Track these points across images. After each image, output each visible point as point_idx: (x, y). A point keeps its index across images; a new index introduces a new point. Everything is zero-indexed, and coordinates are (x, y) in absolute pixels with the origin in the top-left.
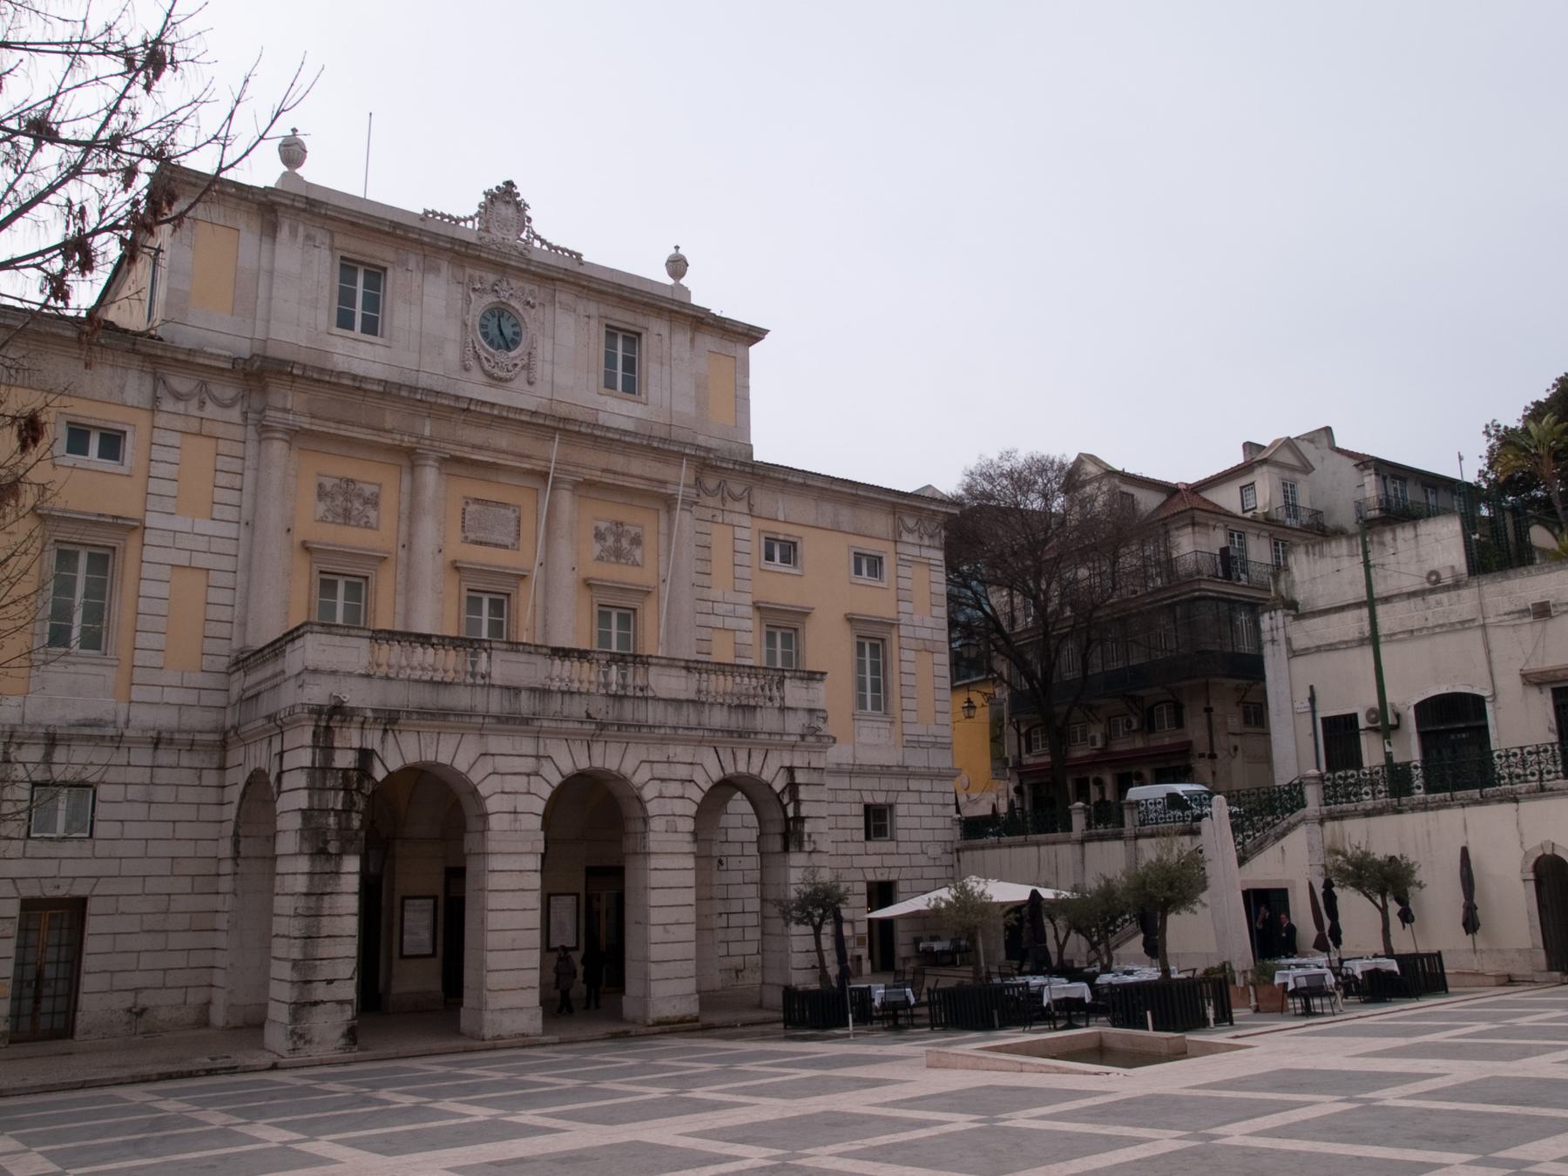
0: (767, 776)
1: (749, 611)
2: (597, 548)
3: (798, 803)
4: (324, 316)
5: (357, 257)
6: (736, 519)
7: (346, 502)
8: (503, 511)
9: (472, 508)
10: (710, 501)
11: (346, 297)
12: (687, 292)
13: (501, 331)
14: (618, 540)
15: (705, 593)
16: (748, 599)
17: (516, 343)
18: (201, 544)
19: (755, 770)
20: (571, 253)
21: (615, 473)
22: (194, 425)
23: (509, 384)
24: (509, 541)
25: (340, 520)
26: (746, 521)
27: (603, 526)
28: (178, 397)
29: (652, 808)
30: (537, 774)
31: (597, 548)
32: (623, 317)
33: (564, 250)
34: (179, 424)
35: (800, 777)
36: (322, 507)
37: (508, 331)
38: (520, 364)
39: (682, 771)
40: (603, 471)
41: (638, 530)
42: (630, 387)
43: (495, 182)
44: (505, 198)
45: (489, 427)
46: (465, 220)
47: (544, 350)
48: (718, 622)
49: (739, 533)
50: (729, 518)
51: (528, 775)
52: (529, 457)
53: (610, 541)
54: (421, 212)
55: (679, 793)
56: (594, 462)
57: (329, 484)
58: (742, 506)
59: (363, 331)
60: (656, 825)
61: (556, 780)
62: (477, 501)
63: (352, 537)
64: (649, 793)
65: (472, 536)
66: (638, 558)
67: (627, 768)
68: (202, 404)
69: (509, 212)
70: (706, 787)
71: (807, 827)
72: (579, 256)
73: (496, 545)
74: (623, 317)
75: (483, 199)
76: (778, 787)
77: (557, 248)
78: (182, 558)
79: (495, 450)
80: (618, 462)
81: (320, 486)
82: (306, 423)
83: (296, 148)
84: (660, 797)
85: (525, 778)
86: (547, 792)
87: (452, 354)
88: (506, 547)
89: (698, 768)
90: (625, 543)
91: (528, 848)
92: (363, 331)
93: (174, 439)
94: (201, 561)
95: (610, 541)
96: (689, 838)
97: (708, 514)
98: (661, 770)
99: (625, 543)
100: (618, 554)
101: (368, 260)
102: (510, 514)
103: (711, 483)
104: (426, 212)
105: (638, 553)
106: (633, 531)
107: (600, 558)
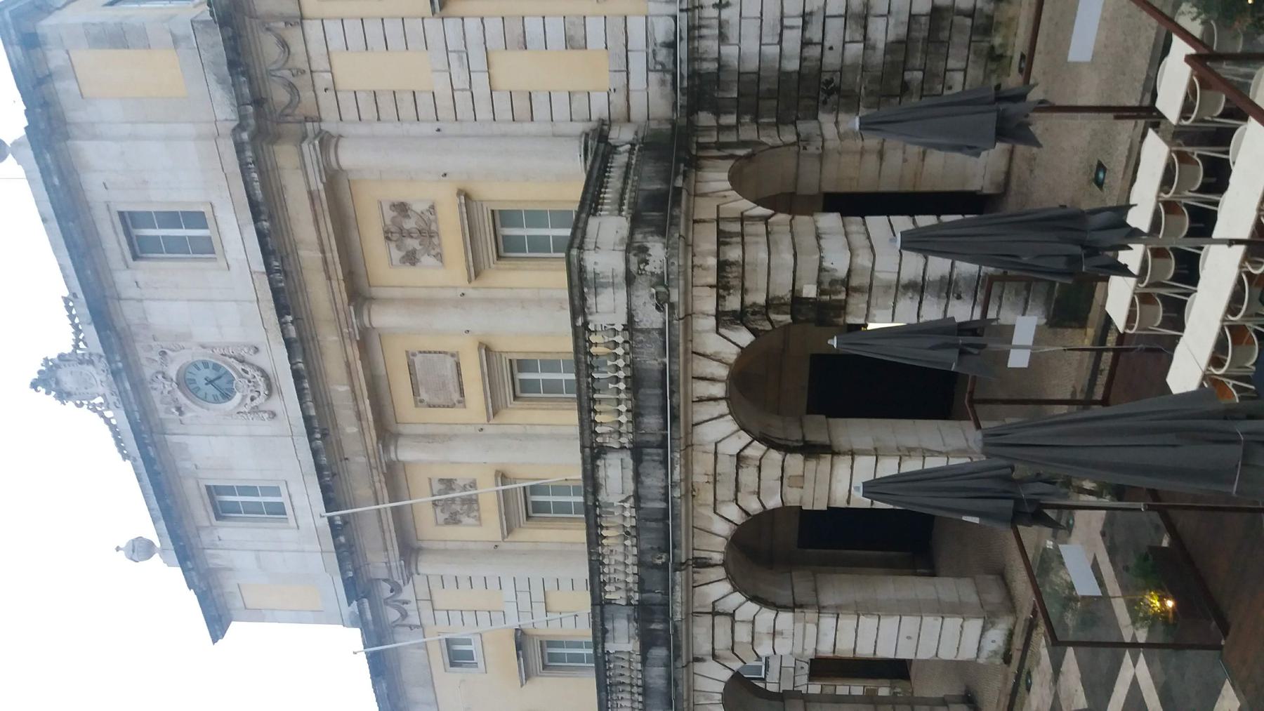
0: (731, 353)
1: (452, 25)
2: (426, 260)
3: (772, 304)
4: (286, 535)
5: (210, 509)
6: (316, 48)
7: (456, 504)
8: (417, 366)
9: (424, 395)
10: (307, 95)
11: (254, 509)
12: (16, 144)
13: (214, 382)
14: (410, 235)
15: (444, 102)
16: (433, 25)
17: (216, 367)
18: (524, 597)
19: (723, 372)
20: (69, 309)
21: (325, 261)
22: (425, 606)
23: (269, 371)
24: (450, 362)
25: (475, 506)
26: (313, 29)
27: (397, 255)
28: (404, 615)
29: (773, 502)
30: (732, 615)
31: (426, 260)
32: (113, 242)
33: (71, 317)
34: (426, 612)
35: (733, 303)
36: (465, 520)
37: (211, 374)
38: (239, 367)
39: (727, 467)
40: (329, 278)
41: (386, 208)
42: (196, 219)
43: (46, 401)
44: (50, 379)
45: (330, 405)
46: (107, 421)
47: (207, 334)
48: (480, 81)
49: (336, 43)
50: (319, 63)
51: (733, 622)
52: (348, 365)
53: (413, 243)
54: (128, 462)
55: (754, 471)
56: (321, 293)
57: (442, 517)
58: (293, 36)
59: (280, 495)
60: (793, 497)
61: (738, 598)
62: (415, 393)
63: (488, 493)
64: (754, 506)
65: (456, 396)
66: (426, 207)
67: (723, 529)
68: (406, 602)
69: (68, 379)
70: (746, 438)
71: (810, 291)
72: (66, 300)
73: (459, 374)
74: (113, 242)
75: (70, 404)
76: (744, 337)
77: (75, 326)
78: (539, 609)
79: (355, 399)
80: (309, 256)
81: (447, 522)
82: (395, 552)
83: (136, 544)
84: (758, 493)
85: (737, 627)
86: (752, 607)
87: (264, 427)
88: (458, 365)
89: (720, 446)
90: (410, 224)
91: (811, 628)
92: (280, 495)
93: (441, 616)
94: (538, 595)
95: (413, 243)
96: (812, 464)
97: (326, 100)
98: (726, 491)
99: (410, 224)
100: (428, 234)
101: (207, 500)
102: (418, 360)
103: (280, 96)
104: (125, 457)
105: (419, 207)
106: (390, 214)
107: (439, 256)
